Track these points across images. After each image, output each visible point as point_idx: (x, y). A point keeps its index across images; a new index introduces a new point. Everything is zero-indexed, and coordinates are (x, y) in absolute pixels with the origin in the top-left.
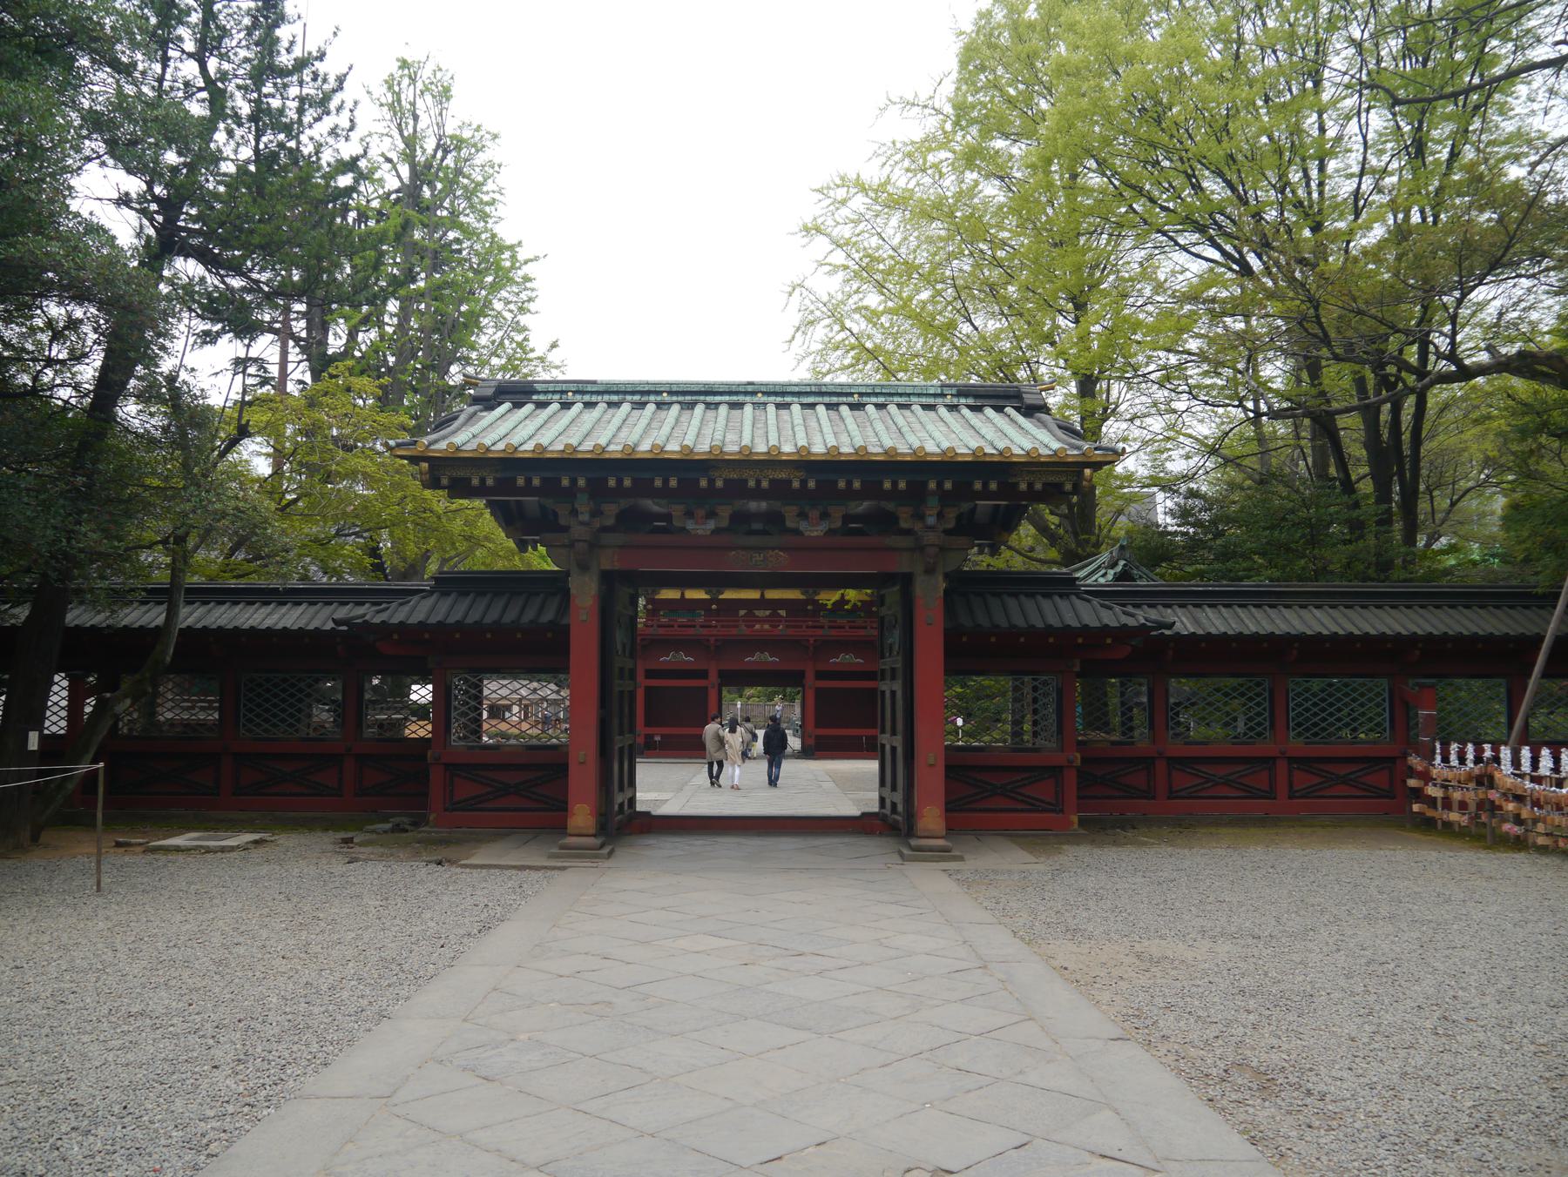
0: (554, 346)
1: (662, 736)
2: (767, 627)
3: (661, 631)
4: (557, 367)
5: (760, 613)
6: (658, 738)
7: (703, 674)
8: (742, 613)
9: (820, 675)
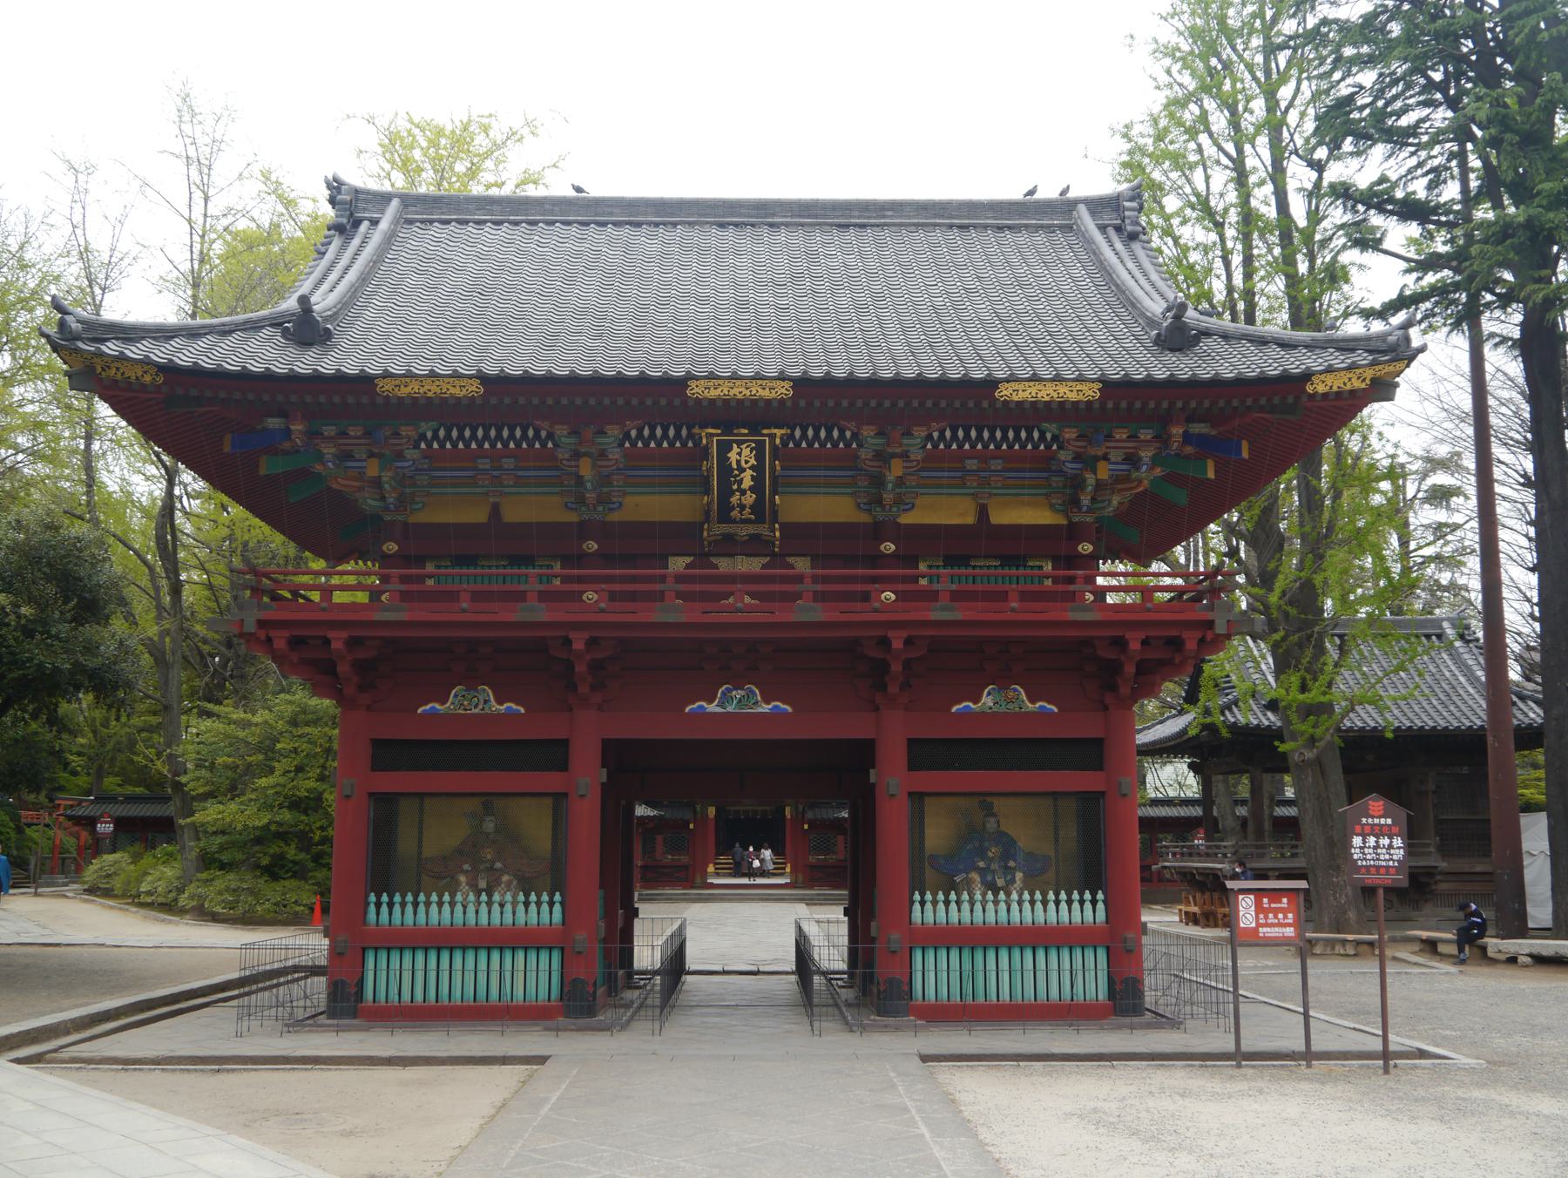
3: (420, 613)
8: (678, 564)
9: (923, 754)
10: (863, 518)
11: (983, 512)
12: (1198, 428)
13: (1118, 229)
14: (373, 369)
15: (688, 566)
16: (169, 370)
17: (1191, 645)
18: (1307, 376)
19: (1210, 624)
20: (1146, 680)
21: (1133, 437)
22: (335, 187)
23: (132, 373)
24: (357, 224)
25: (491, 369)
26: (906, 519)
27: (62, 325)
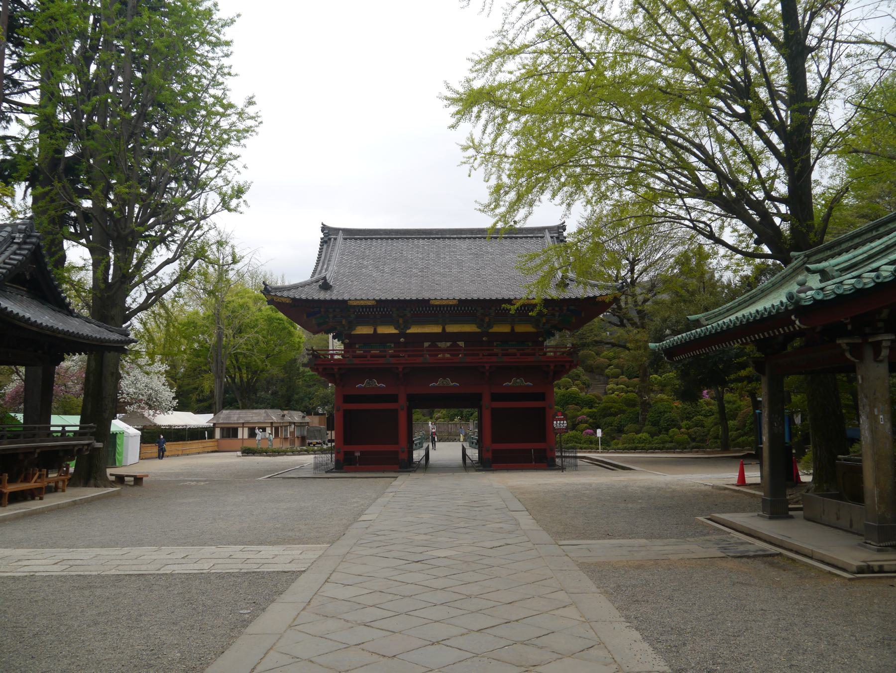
0: (251, 103)
1: (361, 452)
2: (448, 356)
4: (252, 118)
5: (442, 345)
6: (358, 454)
7: (393, 398)
8: (426, 344)
9: (495, 397)
10: (479, 330)
11: (513, 328)
12: (572, 308)
13: (558, 238)
14: (346, 297)
15: (429, 346)
16: (294, 299)
17: (568, 367)
18: (595, 297)
19: (572, 362)
20: (558, 374)
21: (553, 309)
22: (324, 228)
23: (284, 300)
24: (330, 239)
25: (377, 298)
26: (490, 331)
27: (266, 288)
